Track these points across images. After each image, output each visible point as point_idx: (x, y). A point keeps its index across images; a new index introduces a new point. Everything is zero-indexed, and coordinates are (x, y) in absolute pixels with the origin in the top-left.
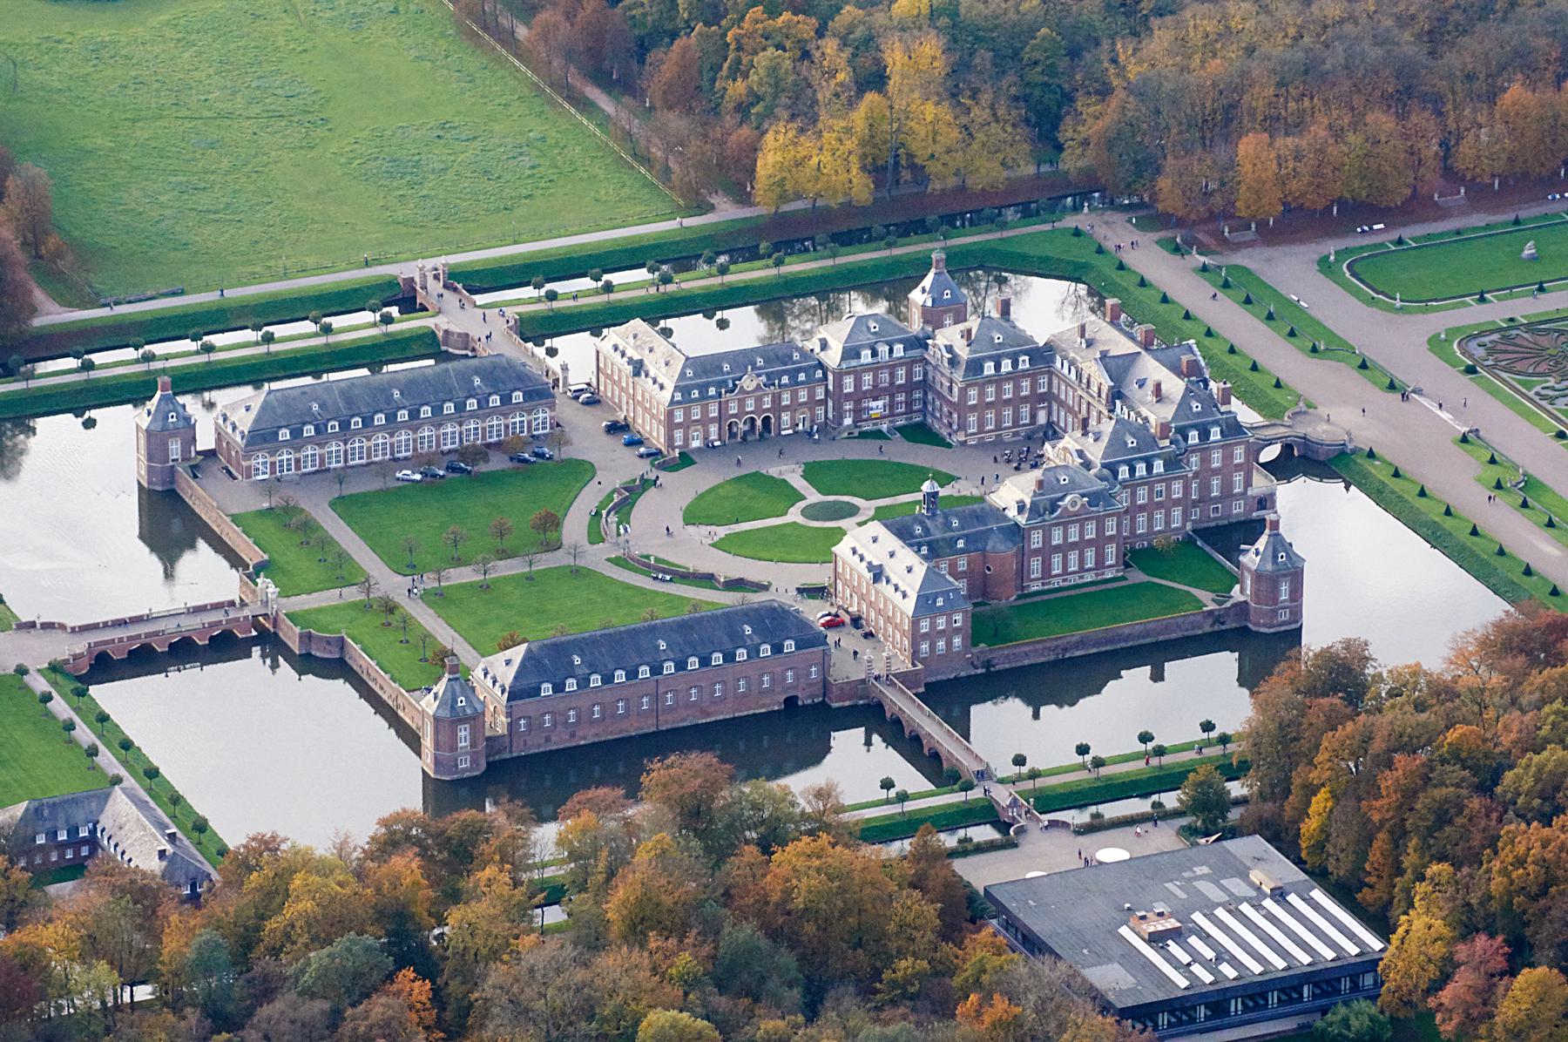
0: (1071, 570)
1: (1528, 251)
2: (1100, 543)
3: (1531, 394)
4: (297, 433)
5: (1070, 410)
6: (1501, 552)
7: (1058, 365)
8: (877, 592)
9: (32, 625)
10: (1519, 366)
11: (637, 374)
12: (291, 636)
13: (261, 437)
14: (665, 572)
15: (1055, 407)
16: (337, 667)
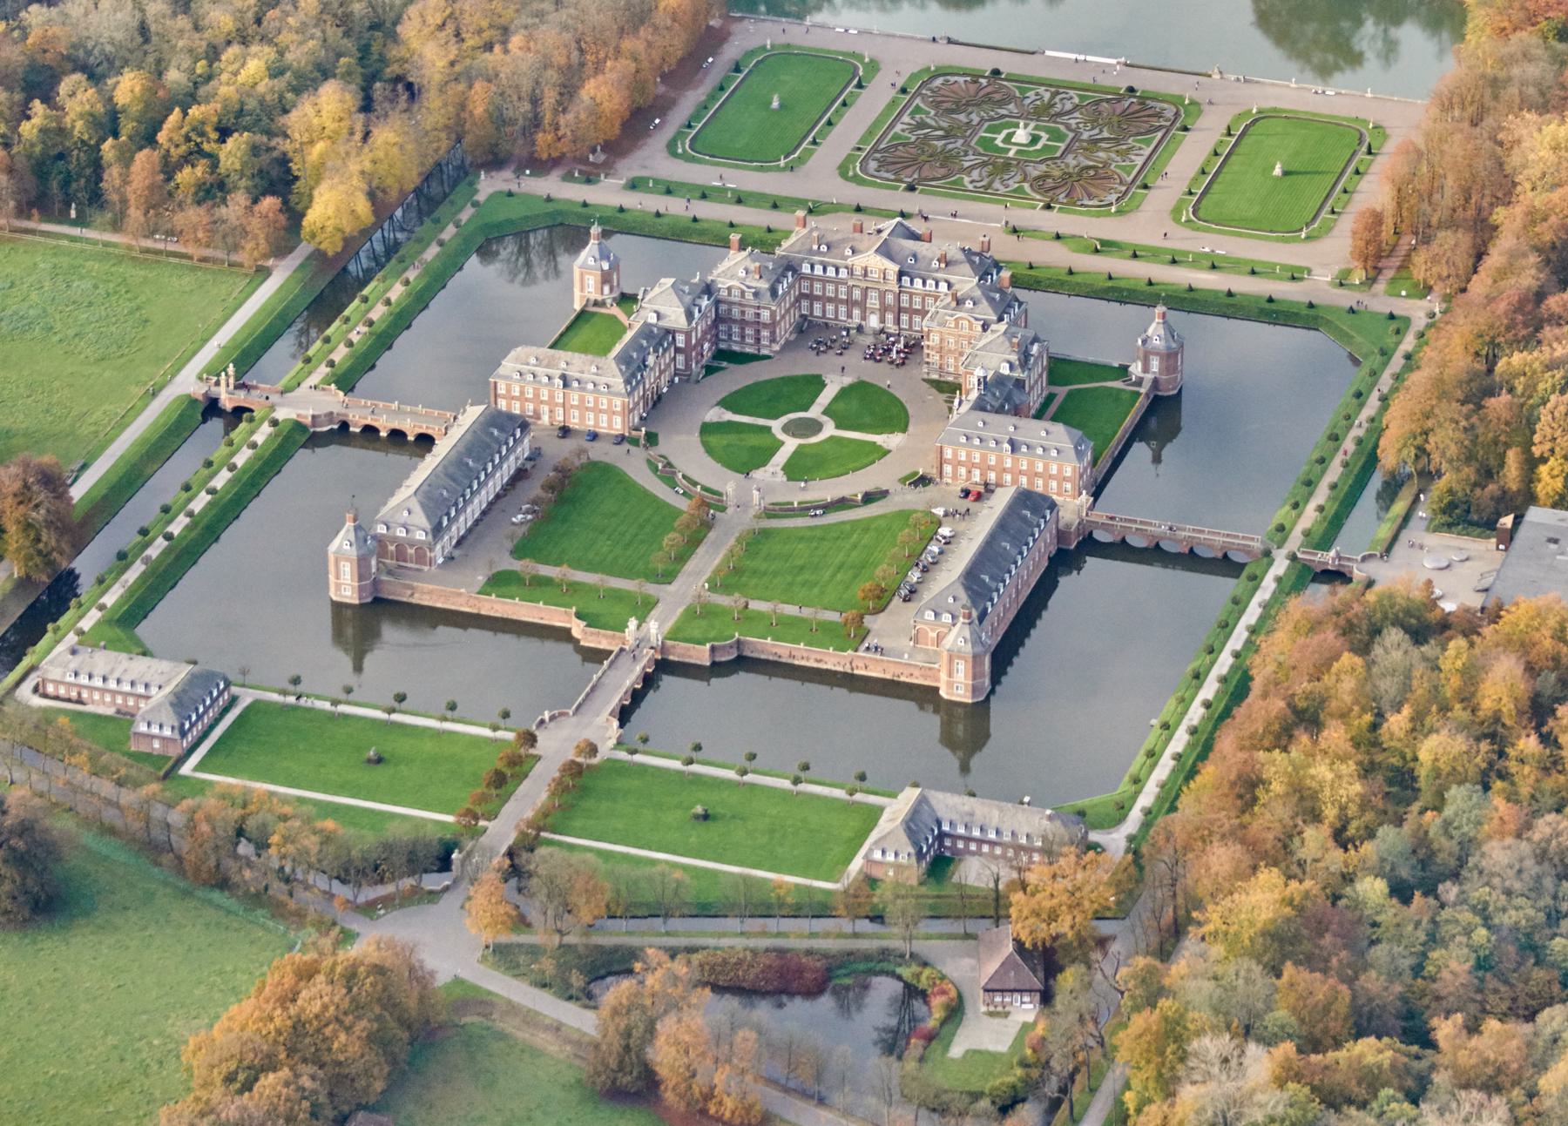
0: (1035, 400)
1: (775, 104)
2: (1041, 376)
3: (970, 187)
4: (448, 514)
5: (835, 300)
6: (1191, 289)
7: (806, 269)
8: (1015, 461)
9: (542, 722)
10: (926, 172)
11: (565, 385)
12: (701, 655)
13: (437, 531)
14: (816, 508)
15: (805, 303)
16: (744, 663)
